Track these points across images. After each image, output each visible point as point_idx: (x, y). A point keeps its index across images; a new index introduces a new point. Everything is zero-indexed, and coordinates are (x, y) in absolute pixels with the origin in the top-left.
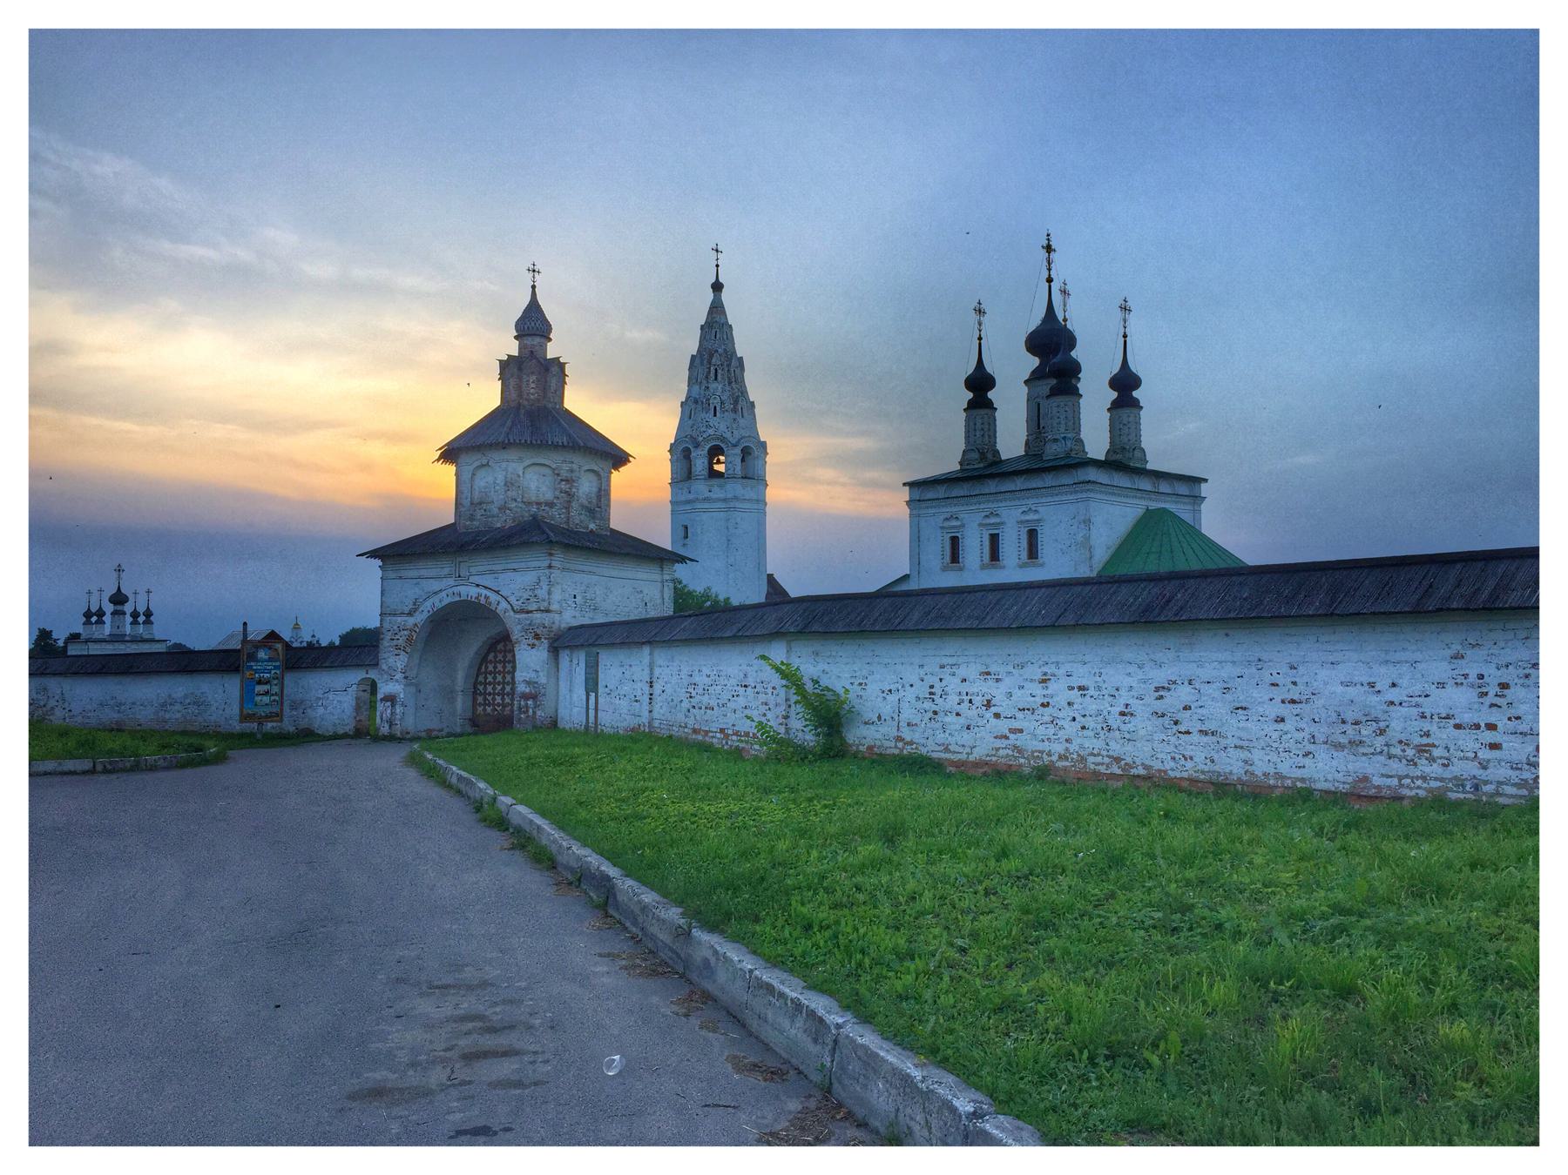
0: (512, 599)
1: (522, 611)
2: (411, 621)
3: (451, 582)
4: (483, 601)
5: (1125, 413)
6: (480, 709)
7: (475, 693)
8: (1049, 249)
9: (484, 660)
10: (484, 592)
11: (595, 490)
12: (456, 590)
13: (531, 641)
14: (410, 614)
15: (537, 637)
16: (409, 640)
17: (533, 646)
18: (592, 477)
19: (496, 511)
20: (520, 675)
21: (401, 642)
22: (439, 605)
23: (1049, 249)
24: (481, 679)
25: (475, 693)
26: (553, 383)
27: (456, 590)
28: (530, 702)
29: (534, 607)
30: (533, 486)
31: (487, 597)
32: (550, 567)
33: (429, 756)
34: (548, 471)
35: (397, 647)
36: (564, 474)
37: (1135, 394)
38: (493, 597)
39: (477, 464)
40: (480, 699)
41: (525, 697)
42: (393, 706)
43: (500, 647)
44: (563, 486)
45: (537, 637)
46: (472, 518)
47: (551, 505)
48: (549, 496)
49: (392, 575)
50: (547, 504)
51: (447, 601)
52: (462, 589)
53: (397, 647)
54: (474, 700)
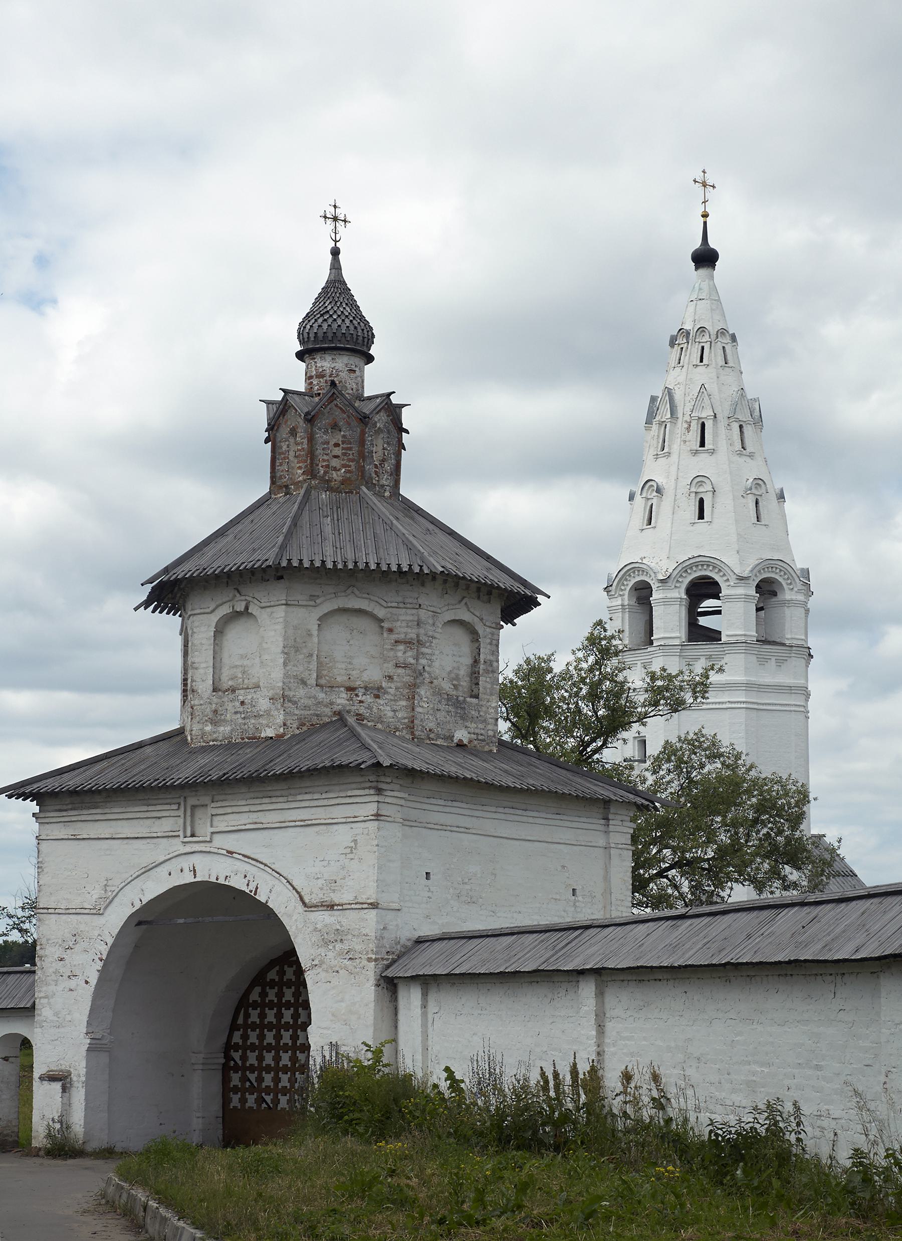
3: (177, 846)
6: (235, 1099)
9: (243, 1004)
11: (468, 661)
18: (461, 636)
19: (264, 704)
25: (226, 1070)
26: (378, 447)
27: (186, 863)
32: (378, 816)
33: (316, 1086)
40: (235, 1079)
43: (272, 975)
44: (402, 654)
46: (216, 718)
47: (377, 692)
48: (373, 674)
49: (58, 831)
52: (198, 861)
54: (226, 1080)
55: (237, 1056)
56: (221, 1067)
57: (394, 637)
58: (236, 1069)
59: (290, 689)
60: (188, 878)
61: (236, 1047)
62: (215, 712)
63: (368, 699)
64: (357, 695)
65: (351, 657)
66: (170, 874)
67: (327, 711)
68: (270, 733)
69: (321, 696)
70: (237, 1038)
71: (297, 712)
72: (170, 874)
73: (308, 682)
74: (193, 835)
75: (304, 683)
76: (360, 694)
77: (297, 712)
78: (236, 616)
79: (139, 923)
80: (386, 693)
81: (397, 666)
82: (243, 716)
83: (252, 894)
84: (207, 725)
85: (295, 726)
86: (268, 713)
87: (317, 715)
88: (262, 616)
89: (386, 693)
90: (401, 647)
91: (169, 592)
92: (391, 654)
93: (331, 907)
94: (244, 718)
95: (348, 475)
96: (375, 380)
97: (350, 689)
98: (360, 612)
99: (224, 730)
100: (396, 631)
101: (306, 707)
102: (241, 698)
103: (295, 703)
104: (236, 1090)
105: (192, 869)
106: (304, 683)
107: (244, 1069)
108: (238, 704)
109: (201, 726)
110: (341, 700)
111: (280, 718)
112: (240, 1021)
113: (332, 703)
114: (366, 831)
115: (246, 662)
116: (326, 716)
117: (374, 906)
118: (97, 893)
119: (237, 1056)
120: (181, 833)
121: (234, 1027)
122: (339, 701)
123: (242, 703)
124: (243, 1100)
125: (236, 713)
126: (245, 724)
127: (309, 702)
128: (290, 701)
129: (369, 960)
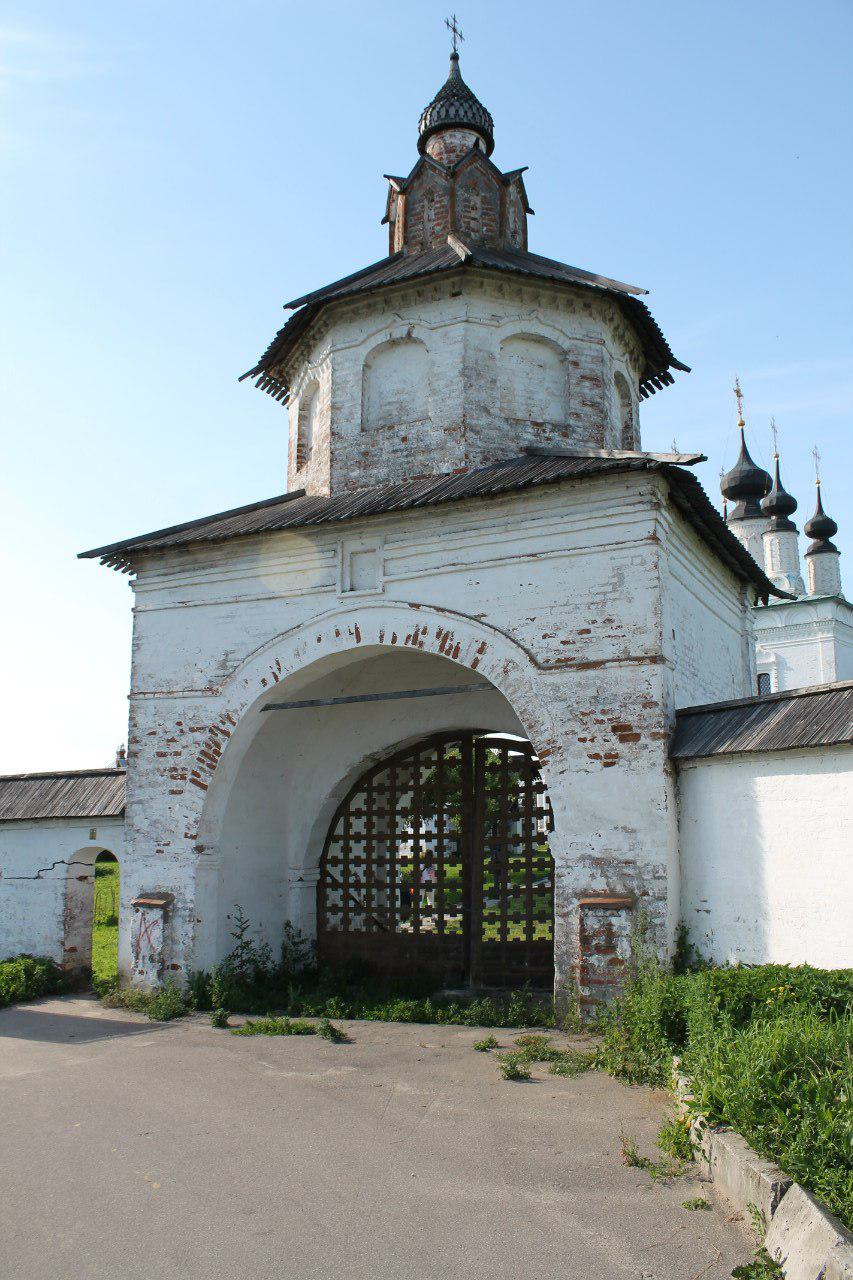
0: (529, 635)
1: (564, 664)
2: (211, 710)
3: (330, 602)
4: (431, 645)
5: (826, 557)
7: (321, 887)
8: (738, 393)
9: (343, 811)
10: (435, 622)
12: (346, 623)
13: (600, 748)
14: (211, 690)
15: (624, 732)
16: (210, 755)
17: (611, 760)
19: (435, 436)
20: (562, 845)
21: (188, 760)
22: (292, 665)
23: (738, 393)
24: (335, 850)
28: (620, 921)
29: (608, 651)
30: (519, 386)
31: (443, 636)
34: (544, 354)
35: (175, 773)
36: (587, 365)
37: (832, 540)
38: (465, 635)
39: (382, 338)
40: (335, 897)
41: (593, 903)
42: (166, 918)
45: (624, 732)
47: (565, 430)
48: (554, 413)
49: (154, 600)
50: (555, 427)
51: (315, 653)
52: (361, 619)
53: (175, 773)
54: (321, 898)
55: (336, 872)
56: (315, 884)
57: (579, 372)
58: (335, 885)
59: (472, 417)
60: (350, 643)
61: (335, 862)
62: (366, 454)
63: (556, 436)
64: (544, 431)
65: (531, 392)
66: (319, 640)
67: (513, 446)
68: (445, 468)
69: (506, 427)
70: (335, 850)
71: (479, 443)
72: (319, 640)
73: (491, 411)
74: (352, 590)
75: (487, 411)
76: (548, 430)
77: (479, 443)
78: (393, 343)
79: (267, 708)
80: (574, 431)
81: (585, 404)
82: (405, 453)
83: (450, 657)
84: (353, 471)
85: (478, 460)
86: (442, 447)
87: (502, 450)
88: (433, 339)
89: (574, 431)
90: (587, 384)
91: (124, 555)
92: (578, 389)
93: (586, 666)
94: (407, 456)
95: (490, 233)
96: (503, 160)
97: (535, 424)
98: (540, 340)
99: (381, 472)
100: (581, 365)
101: (490, 439)
102: (403, 434)
103: (477, 433)
104: (335, 909)
105: (353, 631)
106: (487, 411)
107: (346, 886)
108: (397, 440)
109: (345, 471)
110: (528, 436)
111: (461, 449)
112: (340, 830)
113: (518, 437)
114: (638, 561)
115: (403, 397)
116: (512, 451)
117: (656, 659)
118: (213, 671)
119: (336, 872)
120: (338, 588)
121: (331, 838)
122: (526, 436)
123: (404, 439)
124: (346, 921)
125: (395, 451)
126: (408, 463)
127: (494, 433)
128: (472, 430)
129: (655, 736)
